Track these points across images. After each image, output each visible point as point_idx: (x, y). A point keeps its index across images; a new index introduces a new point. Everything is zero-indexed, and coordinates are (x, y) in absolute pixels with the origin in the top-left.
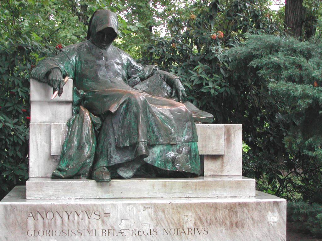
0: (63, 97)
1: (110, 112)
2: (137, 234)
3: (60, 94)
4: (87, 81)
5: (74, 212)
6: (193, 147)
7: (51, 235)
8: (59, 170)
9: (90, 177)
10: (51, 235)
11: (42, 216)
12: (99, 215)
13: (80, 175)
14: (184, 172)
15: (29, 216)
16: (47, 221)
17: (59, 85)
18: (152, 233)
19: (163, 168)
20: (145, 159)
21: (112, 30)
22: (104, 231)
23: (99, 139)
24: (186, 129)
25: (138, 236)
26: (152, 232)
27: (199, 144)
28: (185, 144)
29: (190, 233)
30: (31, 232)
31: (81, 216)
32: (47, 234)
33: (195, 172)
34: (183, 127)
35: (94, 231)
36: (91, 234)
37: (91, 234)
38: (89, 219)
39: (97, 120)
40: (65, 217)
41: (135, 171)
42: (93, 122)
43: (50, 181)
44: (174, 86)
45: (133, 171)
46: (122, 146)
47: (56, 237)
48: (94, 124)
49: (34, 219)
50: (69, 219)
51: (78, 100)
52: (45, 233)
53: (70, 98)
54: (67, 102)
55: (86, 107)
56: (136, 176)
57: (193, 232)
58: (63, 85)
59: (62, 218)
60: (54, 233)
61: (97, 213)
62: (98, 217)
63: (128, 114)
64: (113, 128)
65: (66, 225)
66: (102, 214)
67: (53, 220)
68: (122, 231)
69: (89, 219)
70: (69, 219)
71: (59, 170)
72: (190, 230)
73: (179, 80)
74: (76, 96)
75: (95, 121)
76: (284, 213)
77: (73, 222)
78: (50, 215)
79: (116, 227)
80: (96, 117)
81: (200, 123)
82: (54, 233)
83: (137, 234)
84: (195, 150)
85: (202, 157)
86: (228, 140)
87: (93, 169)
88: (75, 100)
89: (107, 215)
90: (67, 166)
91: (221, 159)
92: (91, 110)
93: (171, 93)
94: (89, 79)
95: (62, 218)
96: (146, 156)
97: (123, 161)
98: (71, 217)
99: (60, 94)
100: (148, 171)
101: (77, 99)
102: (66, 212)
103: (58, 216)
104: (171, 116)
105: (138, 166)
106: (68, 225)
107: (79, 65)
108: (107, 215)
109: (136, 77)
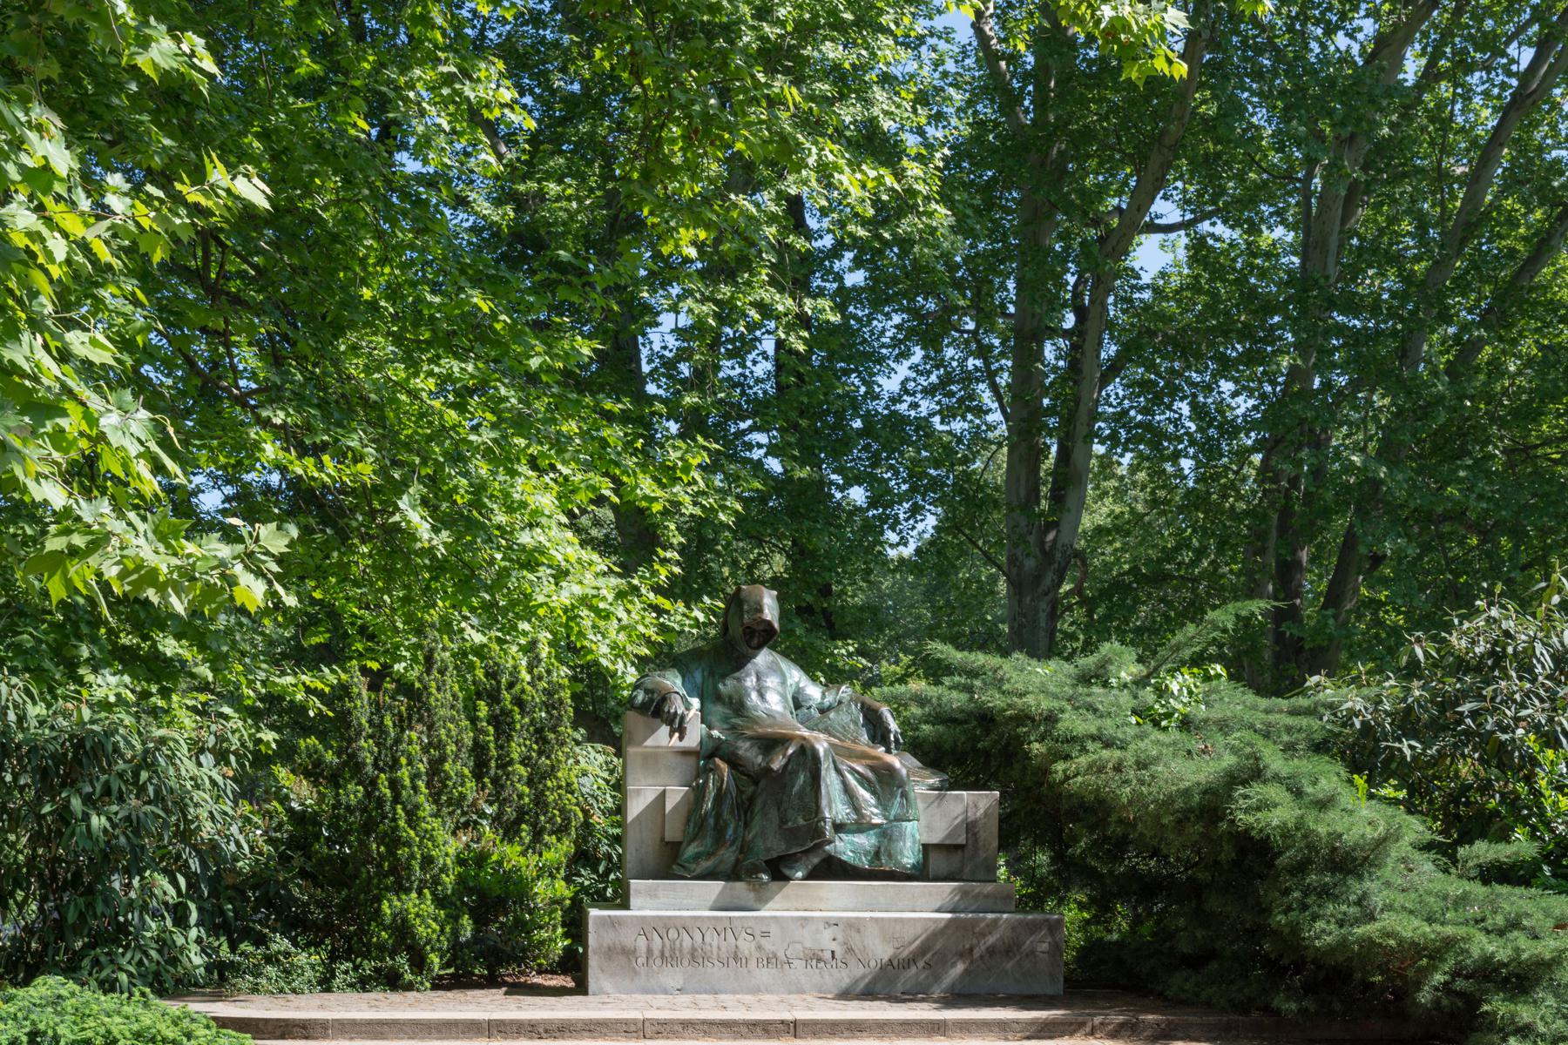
3: (681, 738)
16: (667, 943)
19: (857, 862)
21: (769, 623)
30: (641, 960)
34: (893, 796)
40: (698, 937)
56: (811, 876)
78: (673, 934)
96: (830, 842)
98: (708, 939)
99: (681, 738)
100: (834, 869)
104: (870, 774)
105: (816, 860)
108: (766, 934)
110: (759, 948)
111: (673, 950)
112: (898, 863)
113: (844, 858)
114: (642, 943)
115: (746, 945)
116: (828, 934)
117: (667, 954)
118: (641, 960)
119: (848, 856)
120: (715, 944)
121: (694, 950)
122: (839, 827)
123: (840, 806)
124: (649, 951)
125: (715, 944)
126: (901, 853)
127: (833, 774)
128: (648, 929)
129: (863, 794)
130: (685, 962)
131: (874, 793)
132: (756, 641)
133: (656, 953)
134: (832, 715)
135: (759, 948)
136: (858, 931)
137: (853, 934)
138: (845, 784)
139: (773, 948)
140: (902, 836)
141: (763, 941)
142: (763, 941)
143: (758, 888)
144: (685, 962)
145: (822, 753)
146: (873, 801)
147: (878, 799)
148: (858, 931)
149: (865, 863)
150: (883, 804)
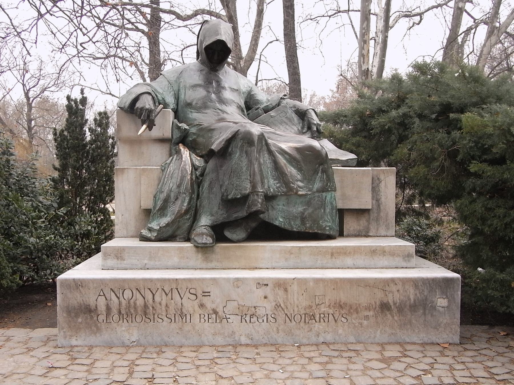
0: (156, 132)
1: (212, 151)
2: (248, 321)
4: (191, 112)
5: (160, 290)
6: (328, 198)
7: (130, 322)
8: (150, 230)
9: (188, 239)
10: (130, 322)
11: (116, 295)
12: (196, 295)
13: (176, 236)
14: (315, 233)
15: (99, 295)
17: (149, 116)
18: (269, 321)
19: (287, 227)
20: (261, 216)
22: (202, 316)
23: (201, 188)
24: (320, 174)
25: (251, 325)
26: (270, 318)
27: (338, 194)
28: (317, 194)
29: (322, 320)
31: (170, 295)
32: (125, 321)
33: (331, 233)
34: (316, 172)
35: (188, 317)
36: (184, 320)
37: (184, 320)
38: (182, 299)
39: (199, 162)
40: (149, 296)
41: (249, 230)
42: (193, 165)
43: (136, 243)
44: (305, 118)
45: (247, 231)
46: (230, 197)
47: (136, 324)
48: (195, 167)
49: (106, 299)
50: (154, 299)
51: (178, 136)
52: (122, 319)
53: (168, 134)
54: (162, 141)
55: (185, 145)
57: (326, 320)
58: (156, 116)
59: (144, 298)
60: (134, 318)
61: (192, 291)
62: (195, 297)
63: (238, 154)
64: (218, 174)
65: (151, 308)
66: (199, 293)
67: (132, 301)
68: (228, 316)
69: (182, 299)
70: (154, 299)
71: (150, 230)
72: (322, 316)
73: (313, 112)
74: (176, 132)
75: (197, 163)
76: (458, 294)
77: (160, 304)
78: (128, 294)
79: (220, 310)
80: (199, 158)
81: (339, 166)
82: (134, 318)
83: (248, 321)
84: (332, 204)
85: (342, 213)
86: (375, 189)
87: (191, 229)
88: (175, 137)
89: (206, 294)
90: (159, 225)
91: (366, 215)
92: (193, 147)
93: (303, 128)
94: (195, 109)
95: (144, 298)
97: (232, 219)
98: (157, 298)
101: (177, 135)
102: (150, 289)
103: (138, 295)
105: (254, 225)
106: (153, 308)
107: (182, 92)
108: (206, 294)
109: (258, 108)
110: (202, 306)
111: (129, 307)
112: (320, 227)
113: (277, 223)
114: (102, 303)
115: (190, 305)
116: (260, 292)
117: (123, 312)
118: (102, 318)
119: (279, 221)
120: (164, 303)
121: (146, 306)
122: (269, 198)
123: (272, 181)
124: (108, 309)
125: (164, 303)
126: (322, 217)
127: (266, 155)
128: (107, 291)
129: (291, 170)
130: (139, 319)
131: (300, 170)
132: (216, 57)
133: (115, 311)
134: (272, 113)
135: (202, 306)
136: (286, 290)
137: (281, 292)
138: (275, 162)
139: (214, 306)
140: (323, 204)
141: (205, 300)
142: (205, 300)
143: (203, 249)
144: (139, 319)
145: (256, 139)
146: (299, 177)
147: (304, 175)
148: (286, 290)
149: (296, 226)
150: (308, 179)
